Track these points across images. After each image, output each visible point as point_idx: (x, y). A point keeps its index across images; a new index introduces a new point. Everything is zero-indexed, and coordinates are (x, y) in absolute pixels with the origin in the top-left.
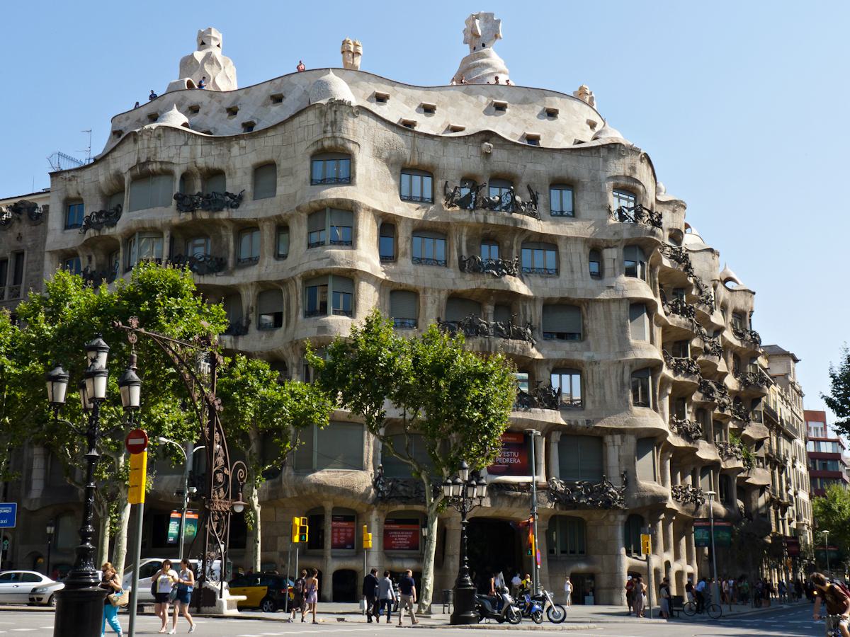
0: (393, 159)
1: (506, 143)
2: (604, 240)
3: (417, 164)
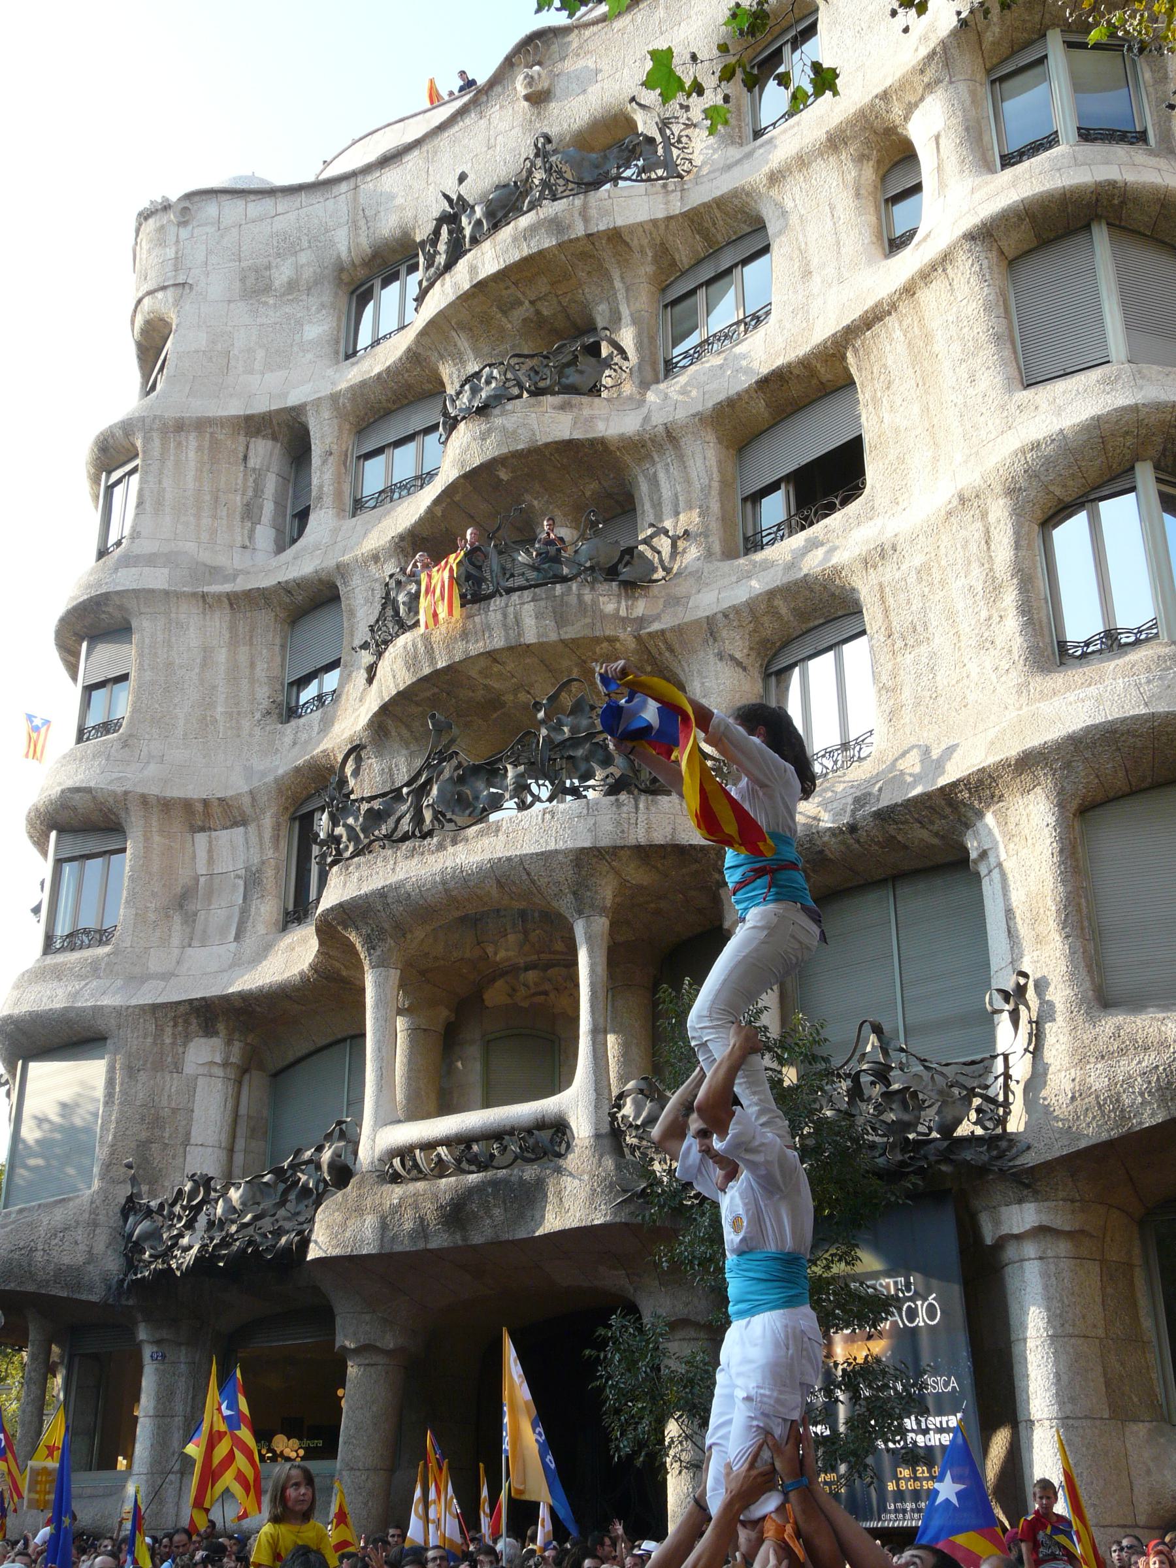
0: (308, 273)
1: (587, 33)
2: (885, 96)
3: (369, 251)
